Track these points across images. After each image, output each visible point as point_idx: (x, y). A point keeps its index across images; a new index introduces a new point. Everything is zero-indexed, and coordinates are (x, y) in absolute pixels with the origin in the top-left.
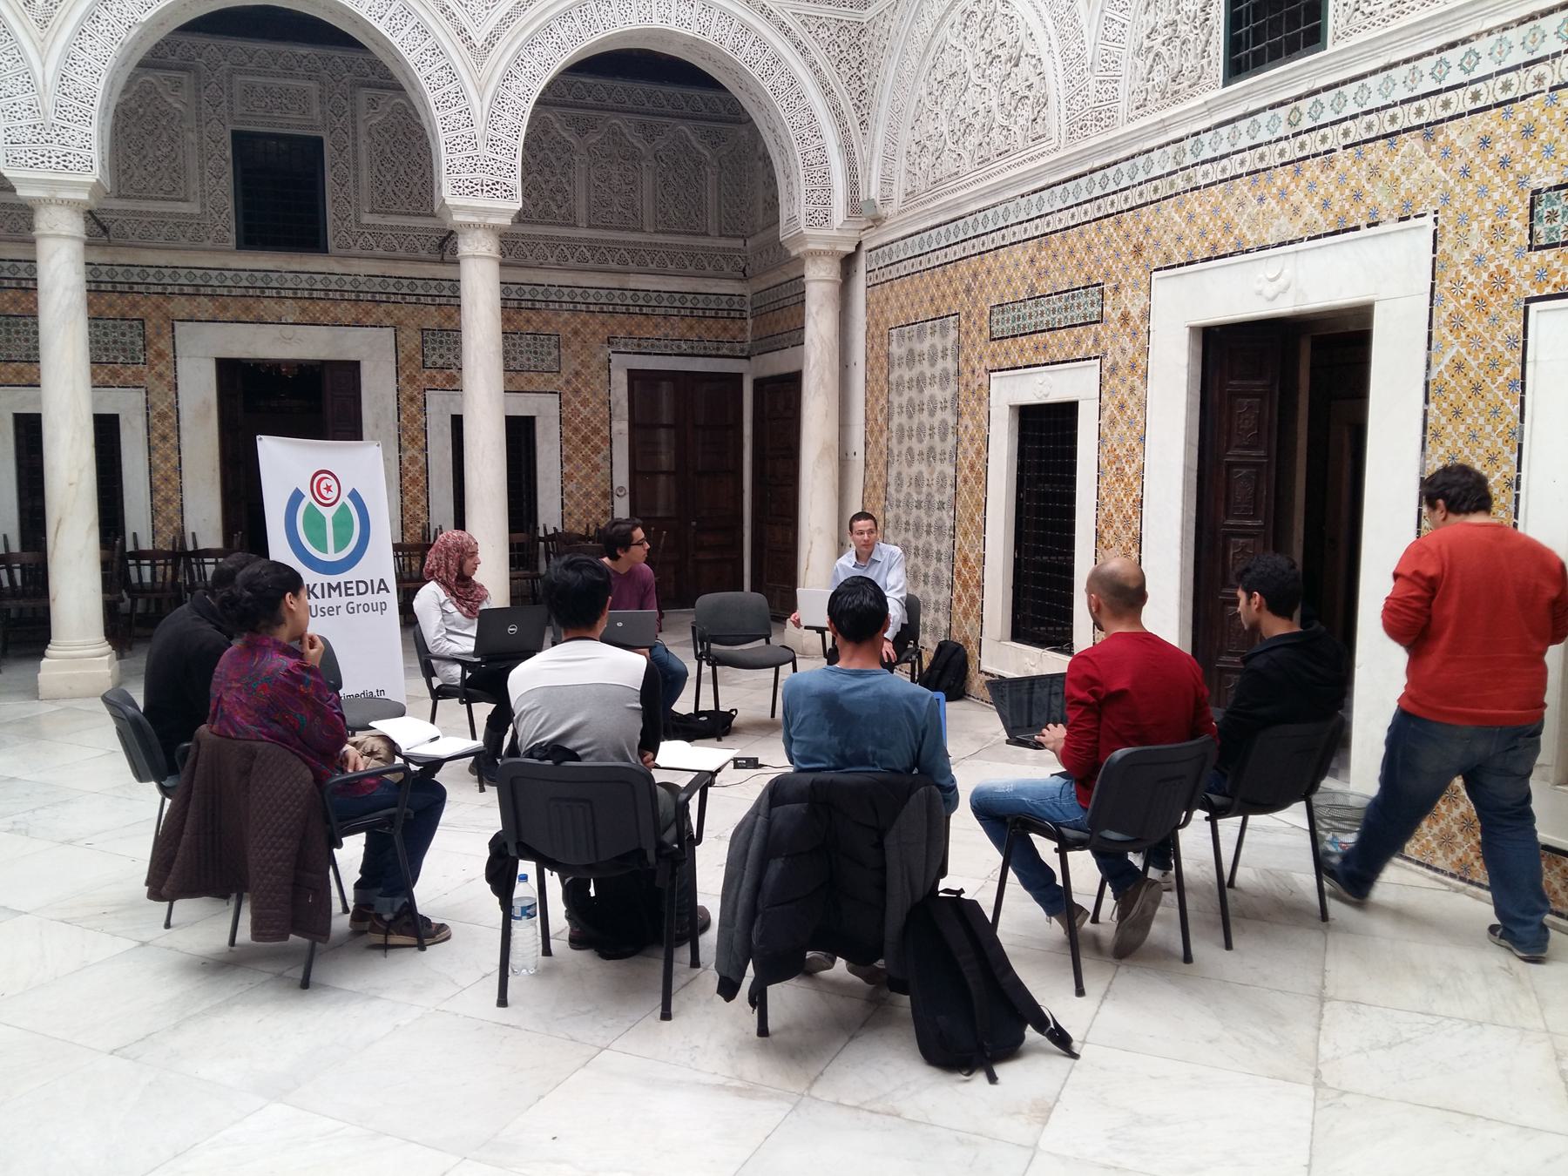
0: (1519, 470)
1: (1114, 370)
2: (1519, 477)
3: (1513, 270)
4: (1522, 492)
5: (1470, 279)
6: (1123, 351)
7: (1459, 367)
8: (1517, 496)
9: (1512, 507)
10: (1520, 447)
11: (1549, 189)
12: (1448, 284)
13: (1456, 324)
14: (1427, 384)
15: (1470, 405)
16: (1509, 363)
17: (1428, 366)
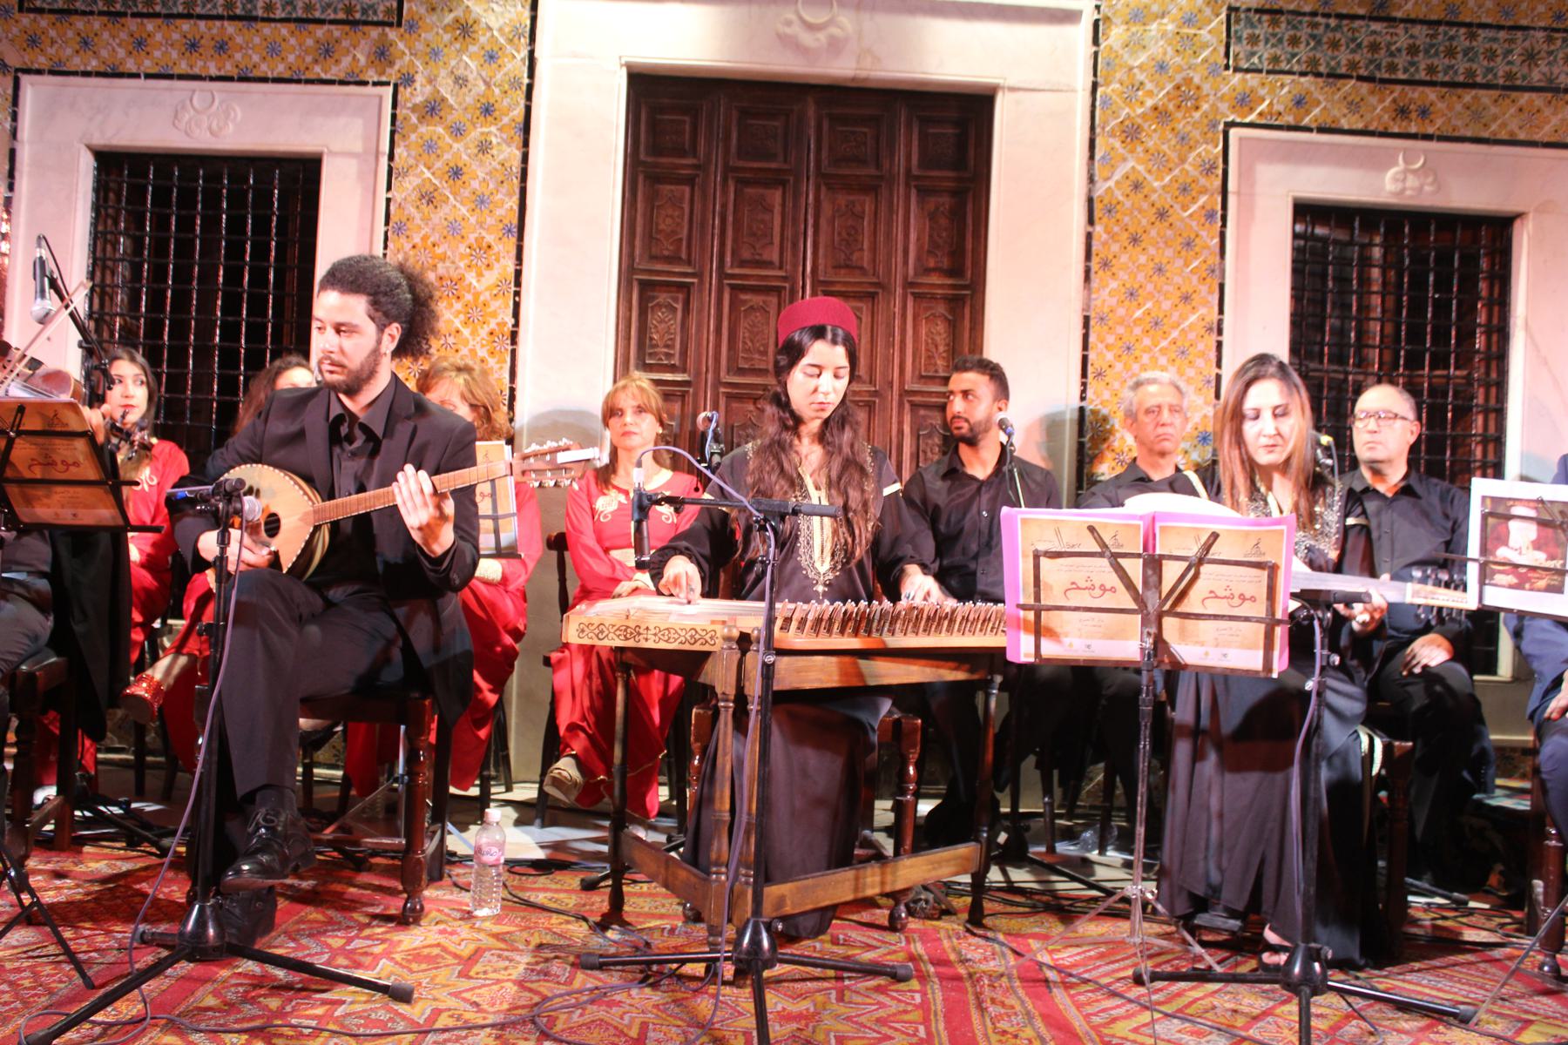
0: (1221, 311)
1: (432, 109)
2: (1220, 322)
3: (1206, 88)
4: (1226, 338)
5: (1149, 86)
6: (461, 82)
7: (1137, 186)
8: (1219, 345)
9: (1213, 355)
10: (1222, 287)
11: (1249, 10)
12: (1116, 86)
13: (1131, 133)
14: (1090, 201)
15: (1153, 233)
16: (1203, 191)
17: (1091, 180)
